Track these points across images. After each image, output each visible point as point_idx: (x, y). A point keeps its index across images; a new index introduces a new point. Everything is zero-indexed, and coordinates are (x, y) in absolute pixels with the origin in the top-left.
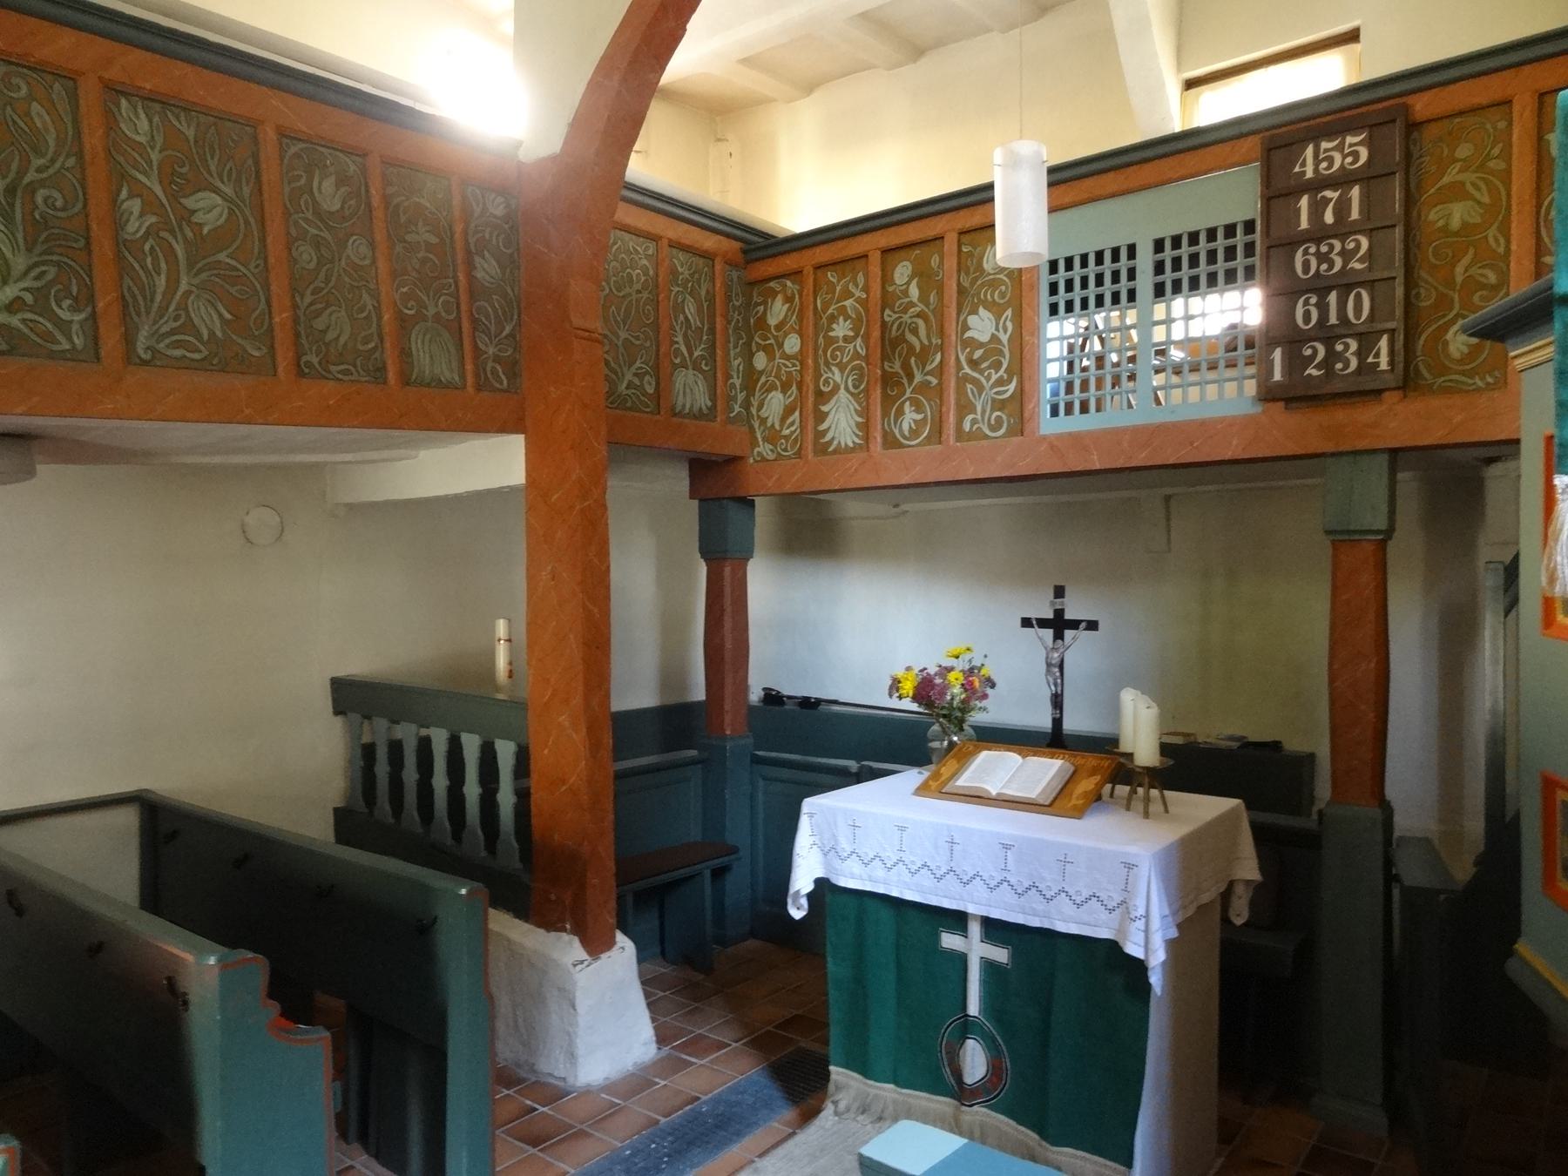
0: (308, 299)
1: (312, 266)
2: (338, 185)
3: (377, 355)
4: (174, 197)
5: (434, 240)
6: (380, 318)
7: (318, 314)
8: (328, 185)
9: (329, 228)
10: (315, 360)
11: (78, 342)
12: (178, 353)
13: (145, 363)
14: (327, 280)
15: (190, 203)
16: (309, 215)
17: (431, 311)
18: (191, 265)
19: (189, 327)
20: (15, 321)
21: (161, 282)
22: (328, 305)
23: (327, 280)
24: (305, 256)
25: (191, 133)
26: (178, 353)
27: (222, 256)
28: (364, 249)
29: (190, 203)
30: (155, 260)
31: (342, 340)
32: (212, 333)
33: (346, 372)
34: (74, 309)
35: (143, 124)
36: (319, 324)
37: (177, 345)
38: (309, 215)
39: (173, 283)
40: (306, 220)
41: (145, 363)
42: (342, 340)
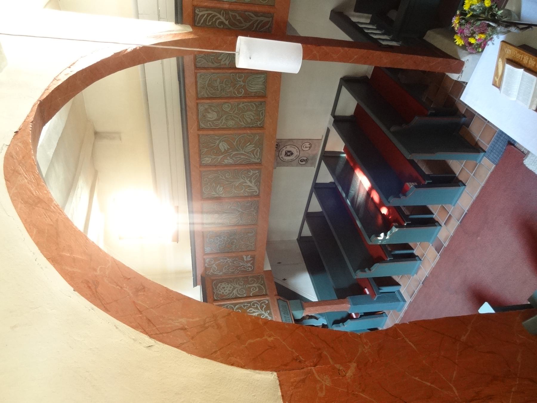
0: (243, 123)
1: (234, 122)
2: (209, 113)
3: (257, 104)
4: (222, 154)
5: (218, 80)
6: (246, 102)
7: (246, 120)
8: (209, 116)
9: (222, 116)
10: (259, 123)
11: (257, 172)
12: (258, 154)
13: (261, 160)
14: (238, 118)
15: (223, 150)
16: (220, 122)
17: (242, 83)
18: (237, 150)
19: (252, 152)
20: (253, 181)
21: (242, 157)
22: (244, 118)
23: (238, 118)
24: (231, 123)
25: (206, 150)
26: (258, 154)
27: (235, 144)
28: (226, 106)
29: (223, 150)
30: (237, 157)
31: (253, 114)
32: (254, 147)
33: (262, 113)
34: (250, 172)
35: (207, 159)
36: (249, 120)
37: (256, 154)
38: (220, 122)
39: (242, 154)
40: (221, 123)
41: (261, 160)
42: (253, 114)
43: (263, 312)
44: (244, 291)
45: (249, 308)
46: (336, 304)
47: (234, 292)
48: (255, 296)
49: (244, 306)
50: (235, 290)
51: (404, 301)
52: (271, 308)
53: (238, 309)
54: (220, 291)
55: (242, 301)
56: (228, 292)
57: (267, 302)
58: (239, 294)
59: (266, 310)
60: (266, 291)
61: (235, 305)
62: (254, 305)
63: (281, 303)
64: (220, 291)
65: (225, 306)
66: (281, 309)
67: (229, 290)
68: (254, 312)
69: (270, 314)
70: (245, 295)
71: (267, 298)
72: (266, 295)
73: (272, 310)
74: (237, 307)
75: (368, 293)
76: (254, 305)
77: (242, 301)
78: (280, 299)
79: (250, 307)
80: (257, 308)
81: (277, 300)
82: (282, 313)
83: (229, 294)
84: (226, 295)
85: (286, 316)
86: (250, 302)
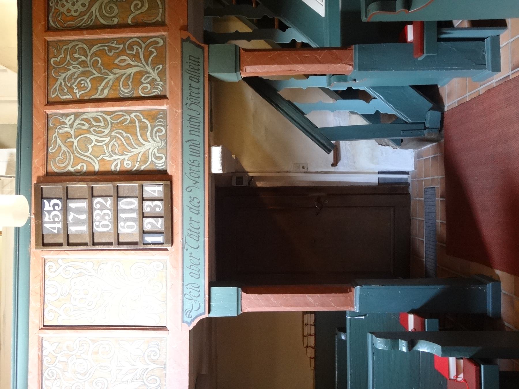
43: (149, 69)
44: (116, 11)
45: (119, 55)
46: (320, 62)
47: (93, 9)
48: (137, 25)
49: (110, 49)
50: (96, 6)
51: (496, 68)
52: (167, 62)
53: (95, 54)
54: (63, 6)
55: (106, 36)
56: (81, 9)
57: (161, 43)
58: (103, 16)
59: (154, 65)
60: (164, 14)
61: (91, 43)
62: (131, 48)
63: (189, 48)
64: (63, 6)
65: (70, 46)
66: (186, 66)
67: (83, 5)
68: (129, 66)
69: (162, 74)
70: (116, 21)
71: (164, 33)
72: (161, 24)
73: (167, 66)
74: (94, 49)
75: (410, 37)
76: (131, 48)
77: (106, 36)
78: (188, 39)
79: (122, 52)
80: (136, 56)
81: (183, 41)
82: (187, 76)
83: (82, 14)
84: (74, 18)
85: (194, 84)
86: (123, 41)
